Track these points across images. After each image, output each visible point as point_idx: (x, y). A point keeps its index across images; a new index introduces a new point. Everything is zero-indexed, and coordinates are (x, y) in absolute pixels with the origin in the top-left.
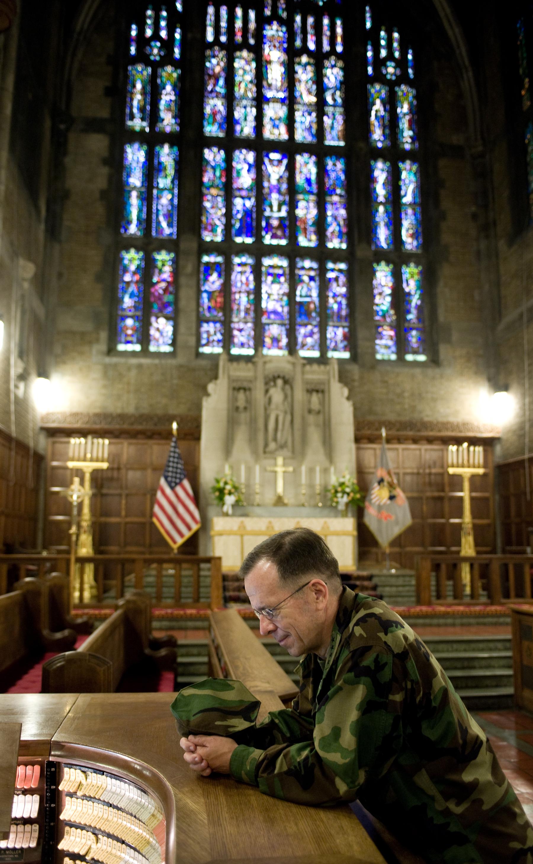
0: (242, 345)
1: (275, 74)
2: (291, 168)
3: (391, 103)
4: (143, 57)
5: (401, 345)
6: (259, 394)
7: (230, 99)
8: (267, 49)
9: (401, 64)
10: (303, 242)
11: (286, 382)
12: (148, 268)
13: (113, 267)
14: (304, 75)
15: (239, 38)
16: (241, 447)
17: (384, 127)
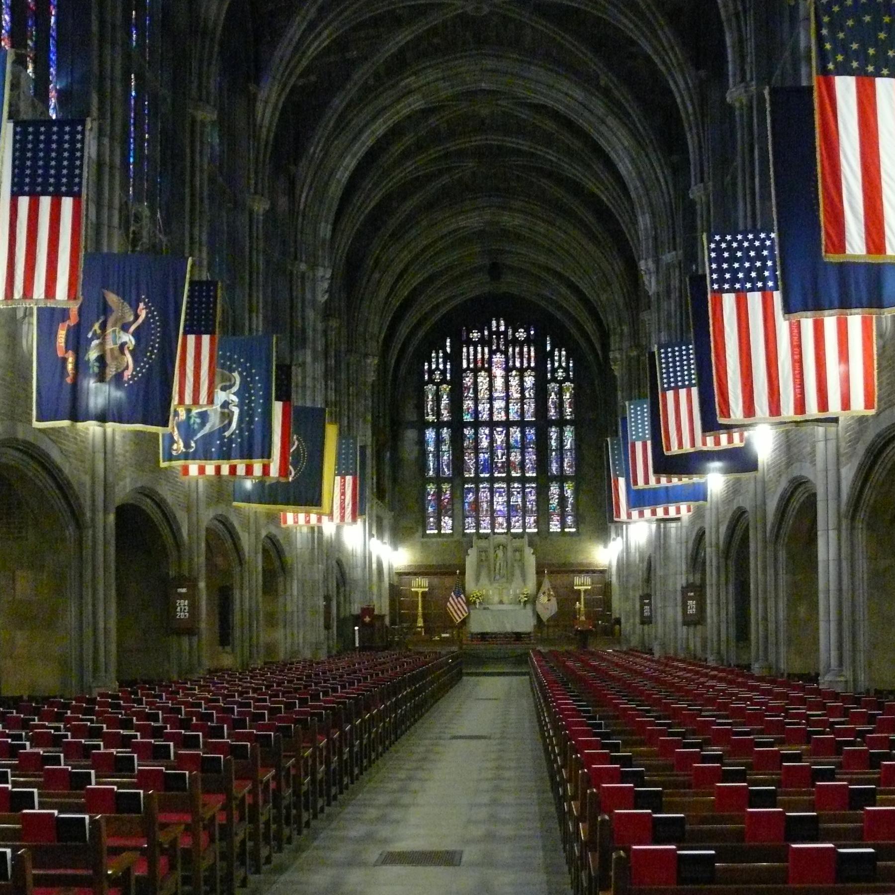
0: (485, 528)
1: (499, 383)
2: (508, 435)
3: (560, 393)
4: (431, 381)
5: (563, 524)
6: (492, 555)
7: (476, 401)
8: (494, 370)
9: (566, 370)
10: (514, 474)
11: (504, 547)
12: (439, 493)
13: (423, 493)
14: (514, 382)
15: (479, 365)
16: (484, 580)
17: (555, 408)
